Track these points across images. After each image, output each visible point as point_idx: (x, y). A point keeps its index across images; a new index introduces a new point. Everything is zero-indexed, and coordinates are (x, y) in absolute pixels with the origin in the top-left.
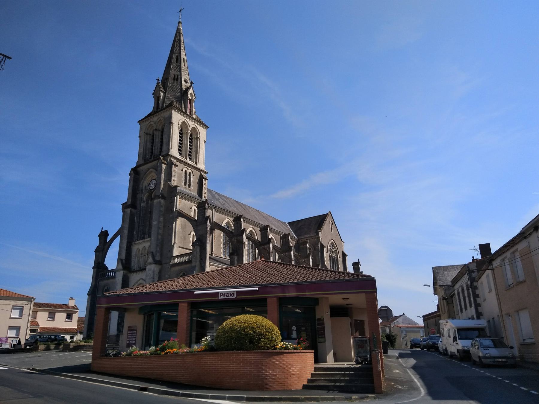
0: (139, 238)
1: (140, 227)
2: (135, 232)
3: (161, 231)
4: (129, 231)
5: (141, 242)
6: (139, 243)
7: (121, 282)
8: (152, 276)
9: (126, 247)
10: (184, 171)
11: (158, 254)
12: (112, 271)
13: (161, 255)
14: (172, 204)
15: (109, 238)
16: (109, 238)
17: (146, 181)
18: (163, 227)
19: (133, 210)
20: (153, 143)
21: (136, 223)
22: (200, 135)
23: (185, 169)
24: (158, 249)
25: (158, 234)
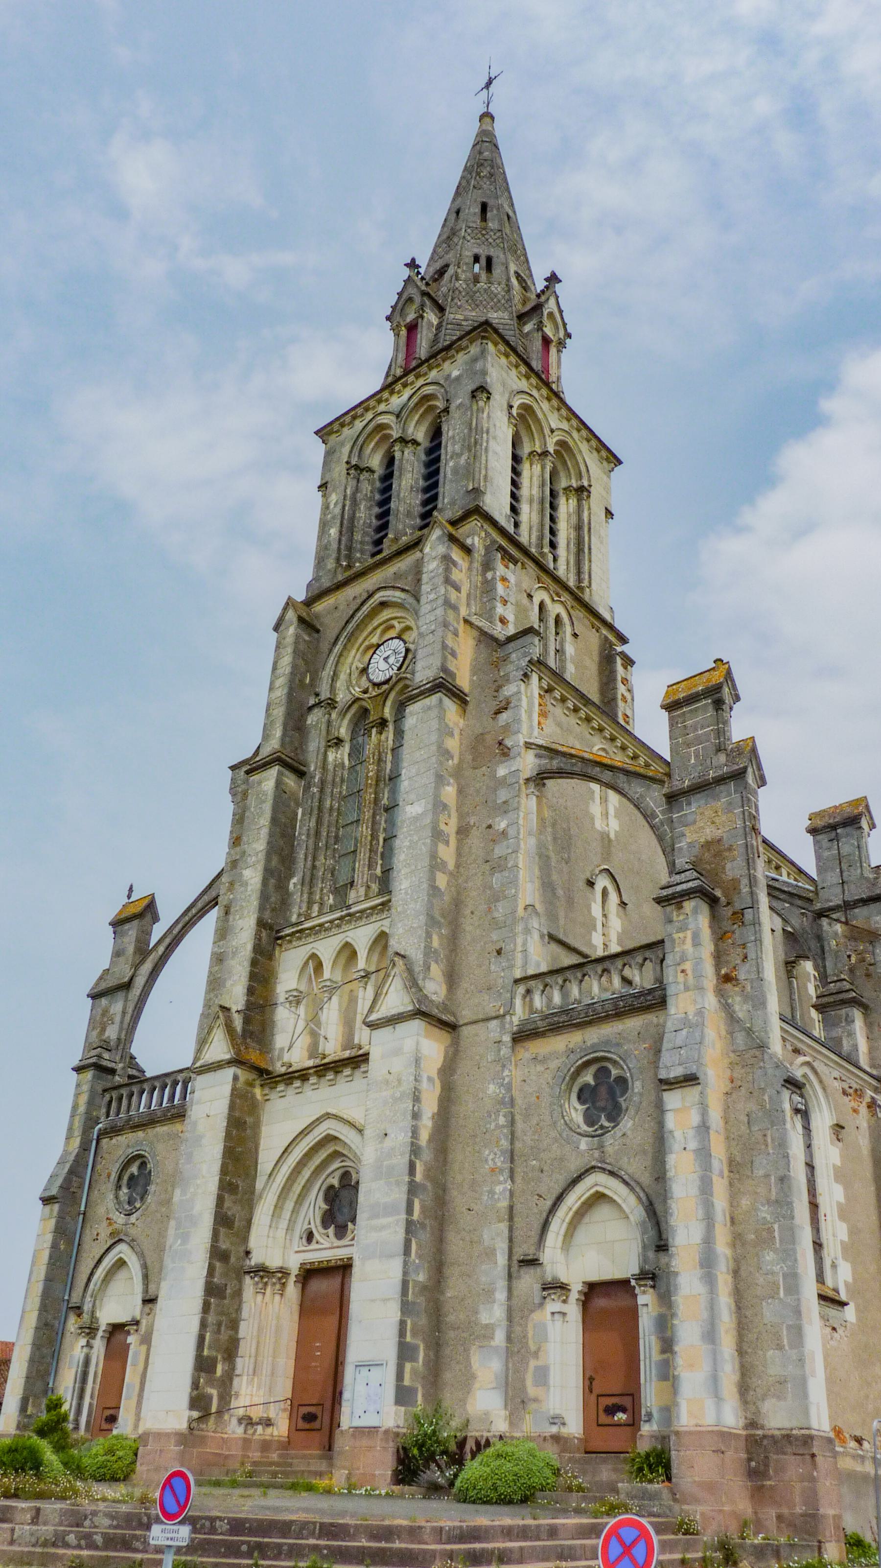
0: (316, 907)
1: (322, 858)
2: (294, 880)
3: (447, 853)
4: (268, 872)
5: (331, 922)
6: (321, 925)
7: (221, 1124)
8: (408, 1085)
9: (249, 947)
10: (536, 600)
11: (436, 970)
12: (166, 1080)
13: (452, 978)
14: (504, 717)
15: (158, 931)
16: (158, 931)
17: (353, 652)
18: (458, 832)
19: (290, 781)
20: (385, 502)
21: (303, 837)
22: (589, 477)
23: (540, 596)
24: (436, 943)
25: (435, 864)
